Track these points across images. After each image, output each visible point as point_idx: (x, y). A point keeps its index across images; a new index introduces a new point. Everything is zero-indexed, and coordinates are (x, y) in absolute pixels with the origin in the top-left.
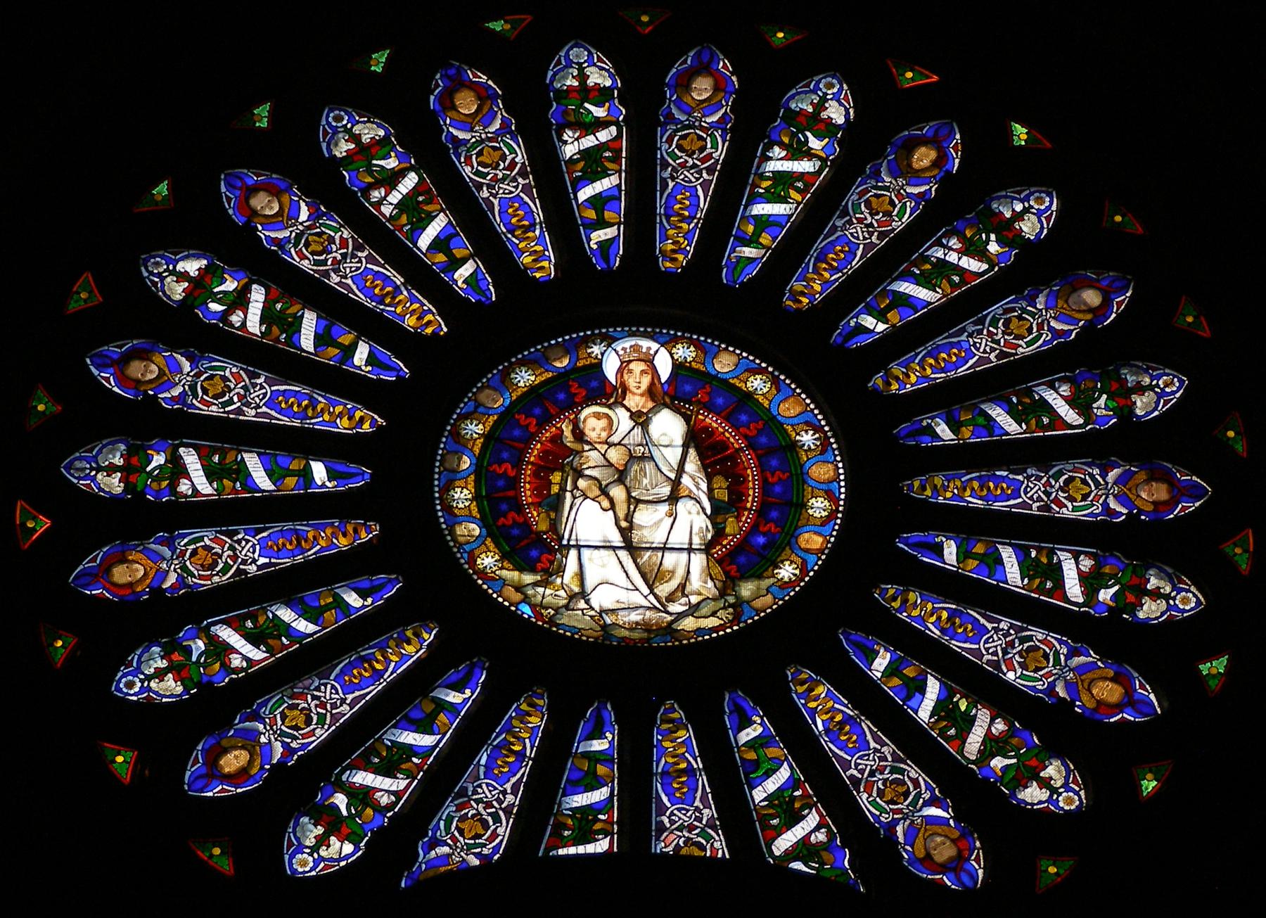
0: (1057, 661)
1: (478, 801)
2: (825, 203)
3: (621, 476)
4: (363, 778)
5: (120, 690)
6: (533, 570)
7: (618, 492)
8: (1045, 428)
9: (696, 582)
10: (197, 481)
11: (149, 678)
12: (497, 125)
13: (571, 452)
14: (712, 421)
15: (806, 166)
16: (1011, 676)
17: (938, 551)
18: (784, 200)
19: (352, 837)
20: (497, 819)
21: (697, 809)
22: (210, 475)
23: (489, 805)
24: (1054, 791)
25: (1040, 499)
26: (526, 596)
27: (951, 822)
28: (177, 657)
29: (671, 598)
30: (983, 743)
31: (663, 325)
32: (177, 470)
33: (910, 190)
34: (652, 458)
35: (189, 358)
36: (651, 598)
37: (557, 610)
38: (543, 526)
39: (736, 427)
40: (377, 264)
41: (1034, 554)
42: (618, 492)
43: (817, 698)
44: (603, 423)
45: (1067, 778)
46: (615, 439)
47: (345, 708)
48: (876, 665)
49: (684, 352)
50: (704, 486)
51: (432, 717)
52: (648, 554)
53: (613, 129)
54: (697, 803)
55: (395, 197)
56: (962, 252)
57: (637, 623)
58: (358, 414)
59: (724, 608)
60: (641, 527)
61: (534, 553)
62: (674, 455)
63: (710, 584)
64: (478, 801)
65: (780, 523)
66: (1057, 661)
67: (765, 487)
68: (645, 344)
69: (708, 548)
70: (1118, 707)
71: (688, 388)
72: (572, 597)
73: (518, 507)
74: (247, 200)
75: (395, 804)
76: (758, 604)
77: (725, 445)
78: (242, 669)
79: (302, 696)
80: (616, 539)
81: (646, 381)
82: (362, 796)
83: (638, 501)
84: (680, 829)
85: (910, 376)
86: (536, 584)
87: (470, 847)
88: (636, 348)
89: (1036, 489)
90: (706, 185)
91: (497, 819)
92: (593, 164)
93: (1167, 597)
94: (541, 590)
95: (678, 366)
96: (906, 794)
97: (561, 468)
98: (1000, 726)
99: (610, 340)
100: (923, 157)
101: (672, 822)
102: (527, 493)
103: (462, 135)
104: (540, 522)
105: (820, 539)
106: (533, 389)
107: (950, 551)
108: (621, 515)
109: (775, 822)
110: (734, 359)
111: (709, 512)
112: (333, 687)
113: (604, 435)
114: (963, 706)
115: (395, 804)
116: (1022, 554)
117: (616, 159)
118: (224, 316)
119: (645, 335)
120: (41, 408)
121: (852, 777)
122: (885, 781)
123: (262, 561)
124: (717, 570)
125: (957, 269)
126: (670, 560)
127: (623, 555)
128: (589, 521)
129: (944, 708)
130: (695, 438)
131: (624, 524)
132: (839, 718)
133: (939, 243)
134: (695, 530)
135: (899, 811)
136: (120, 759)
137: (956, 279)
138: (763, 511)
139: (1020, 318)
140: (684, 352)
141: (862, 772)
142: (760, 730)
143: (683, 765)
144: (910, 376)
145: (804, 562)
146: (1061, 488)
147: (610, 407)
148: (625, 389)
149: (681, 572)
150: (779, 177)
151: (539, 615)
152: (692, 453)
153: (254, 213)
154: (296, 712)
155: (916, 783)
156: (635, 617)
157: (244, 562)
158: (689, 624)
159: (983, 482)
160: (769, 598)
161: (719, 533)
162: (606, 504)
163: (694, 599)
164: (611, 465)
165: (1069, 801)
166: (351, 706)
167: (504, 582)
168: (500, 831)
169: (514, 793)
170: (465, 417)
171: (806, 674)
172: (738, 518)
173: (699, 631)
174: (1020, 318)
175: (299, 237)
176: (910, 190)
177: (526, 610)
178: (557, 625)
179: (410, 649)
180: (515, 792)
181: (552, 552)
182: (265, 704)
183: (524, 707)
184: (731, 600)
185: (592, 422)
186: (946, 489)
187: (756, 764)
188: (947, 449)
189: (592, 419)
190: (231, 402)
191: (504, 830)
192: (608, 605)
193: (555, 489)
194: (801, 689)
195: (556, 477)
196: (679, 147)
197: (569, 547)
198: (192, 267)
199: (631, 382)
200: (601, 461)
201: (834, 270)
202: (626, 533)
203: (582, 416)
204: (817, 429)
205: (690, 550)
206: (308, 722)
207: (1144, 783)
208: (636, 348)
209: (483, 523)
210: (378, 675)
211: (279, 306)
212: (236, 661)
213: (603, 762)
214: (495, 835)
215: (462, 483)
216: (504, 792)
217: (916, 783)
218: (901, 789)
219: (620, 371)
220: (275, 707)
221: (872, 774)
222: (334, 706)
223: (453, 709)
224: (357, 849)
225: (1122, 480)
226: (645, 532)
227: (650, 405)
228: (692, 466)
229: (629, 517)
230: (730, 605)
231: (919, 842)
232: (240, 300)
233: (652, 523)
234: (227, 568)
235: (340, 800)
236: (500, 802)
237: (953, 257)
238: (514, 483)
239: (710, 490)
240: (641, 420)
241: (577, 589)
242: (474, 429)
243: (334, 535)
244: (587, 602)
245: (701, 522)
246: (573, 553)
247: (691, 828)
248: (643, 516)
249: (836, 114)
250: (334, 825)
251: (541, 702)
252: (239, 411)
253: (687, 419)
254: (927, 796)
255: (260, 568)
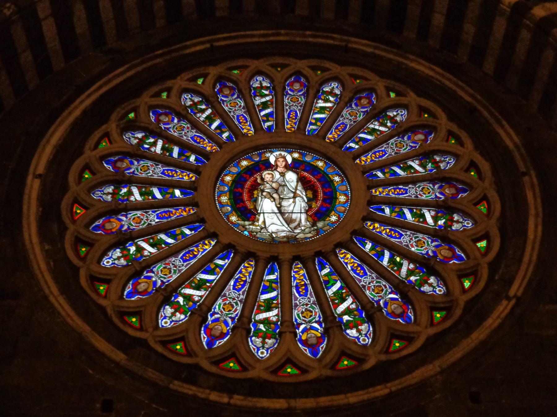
0: (428, 245)
1: (230, 298)
2: (336, 114)
3: (276, 191)
4: (188, 291)
5: (104, 264)
6: (248, 220)
7: (275, 196)
8: (413, 173)
9: (303, 222)
10: (137, 196)
11: (115, 260)
12: (236, 96)
13: (260, 184)
14: (306, 174)
15: (329, 105)
16: (413, 249)
17: (383, 211)
18: (324, 113)
19: (185, 313)
20: (237, 304)
21: (309, 298)
22: (141, 194)
23: (234, 299)
24: (434, 287)
25: (414, 194)
26: (246, 229)
27: (400, 300)
28: (125, 253)
29: (295, 228)
30: (407, 272)
31: (288, 146)
32: (130, 193)
33: (362, 110)
34: (286, 185)
35: (136, 160)
36: (289, 228)
37: (257, 233)
38: (252, 207)
39: (313, 176)
40: (198, 133)
41: (415, 211)
42: (275, 196)
43: (347, 259)
44: (270, 176)
45: (438, 283)
46: (275, 180)
47: (183, 267)
48: (367, 246)
49: (296, 155)
50: (304, 194)
51: (214, 269)
52: (287, 214)
53: (271, 97)
54: (309, 296)
55: (204, 116)
56: (380, 126)
57: (284, 236)
58: (191, 175)
59: (314, 230)
60: (284, 206)
61: (249, 215)
62: (294, 184)
63: (308, 223)
64: (230, 298)
65: (330, 203)
66: (428, 245)
67: (324, 193)
68: (283, 153)
69: (307, 212)
70: (451, 259)
71: (297, 165)
72: (262, 228)
73: (243, 201)
74: (158, 117)
75: (200, 300)
76: (325, 228)
77: (310, 181)
78: (148, 256)
79: (168, 264)
80: (276, 210)
81: (284, 164)
82: (188, 298)
83: (283, 199)
84: (303, 305)
85: (366, 160)
86: (249, 225)
87: (227, 315)
88: (280, 154)
89: (413, 191)
90: (299, 110)
91: (237, 304)
92: (265, 105)
93: (462, 223)
94: (251, 227)
95: (294, 159)
96: (382, 290)
97: (257, 189)
98: (412, 266)
99: (272, 152)
100: (364, 101)
101: (300, 303)
102: (245, 197)
103: (224, 99)
104: (250, 205)
105: (344, 208)
106: (247, 167)
107: (387, 210)
108: (277, 203)
109: (337, 301)
110: (311, 157)
111: (306, 201)
112: (180, 261)
113: (271, 179)
114: (398, 259)
115: (200, 300)
116: (411, 211)
117: (272, 104)
118: (148, 149)
119: (283, 151)
120: (86, 176)
121: (362, 285)
122: (374, 286)
123: (157, 220)
124: (310, 219)
125: (379, 130)
126: (294, 216)
127: (278, 215)
128: (267, 205)
129: (392, 260)
130: (301, 180)
131: (279, 206)
132: (356, 265)
133: (372, 123)
134: (302, 206)
135: (380, 296)
136: (102, 288)
137: (379, 133)
138: (324, 200)
139: (400, 143)
140: (296, 155)
141: (366, 283)
142: (329, 270)
143: (303, 283)
144: (366, 160)
145: (339, 215)
146: (421, 191)
147: (272, 171)
148: (277, 166)
149: (298, 220)
150: (322, 108)
151: (251, 235)
152: (300, 184)
153: (160, 120)
154: (166, 269)
155: (385, 286)
156: (283, 234)
157: (151, 221)
158: (301, 236)
159: (395, 189)
160: (328, 227)
161: (310, 207)
162: (272, 200)
163: (303, 228)
164: (273, 188)
165: (440, 291)
166: (186, 266)
167: (239, 225)
168: (238, 308)
169: (243, 294)
170: (226, 175)
171: (343, 251)
172: (316, 203)
173: (306, 238)
174: (400, 143)
175: (174, 127)
176: (362, 110)
177: (246, 233)
178: (257, 238)
179: (206, 247)
180: (243, 294)
181: (255, 215)
182: (155, 267)
183: (246, 265)
184: (315, 228)
185: (267, 176)
186: (383, 192)
187: (327, 282)
188: (382, 180)
189: (267, 175)
190: (149, 173)
191: (239, 308)
192: (274, 230)
193: (255, 196)
194: (342, 256)
195: (256, 192)
196: (291, 101)
197: (260, 213)
198: (140, 135)
199: (279, 164)
200: (270, 187)
201: (340, 132)
202: (279, 208)
203: (263, 175)
204: (339, 176)
205: (301, 213)
206: (170, 272)
207: (465, 284)
208: (280, 154)
209: (231, 207)
210: (195, 256)
211: (167, 146)
212: (146, 253)
213: (275, 283)
214: (236, 310)
215: (225, 195)
216: (239, 295)
217: (385, 286)
218: (380, 289)
219: (276, 161)
220: (159, 267)
221: (369, 283)
222: (180, 267)
223: (221, 267)
224: (186, 316)
225: (440, 187)
226: (286, 208)
227: (285, 170)
228: (300, 188)
229: (280, 204)
230: (316, 230)
231: (389, 307)
232: (154, 144)
233: (288, 205)
234: (145, 223)
235: (181, 300)
236: (238, 298)
237: (377, 127)
238: (241, 194)
239: (306, 195)
240: (283, 175)
241: (263, 226)
242: (228, 178)
243: (182, 212)
244: (267, 230)
245: (304, 204)
246: (262, 215)
247: (307, 305)
248: (284, 203)
249: (338, 92)
250: (178, 309)
251: (252, 263)
252: (152, 175)
253: (297, 173)
254: (390, 290)
255: (156, 223)
